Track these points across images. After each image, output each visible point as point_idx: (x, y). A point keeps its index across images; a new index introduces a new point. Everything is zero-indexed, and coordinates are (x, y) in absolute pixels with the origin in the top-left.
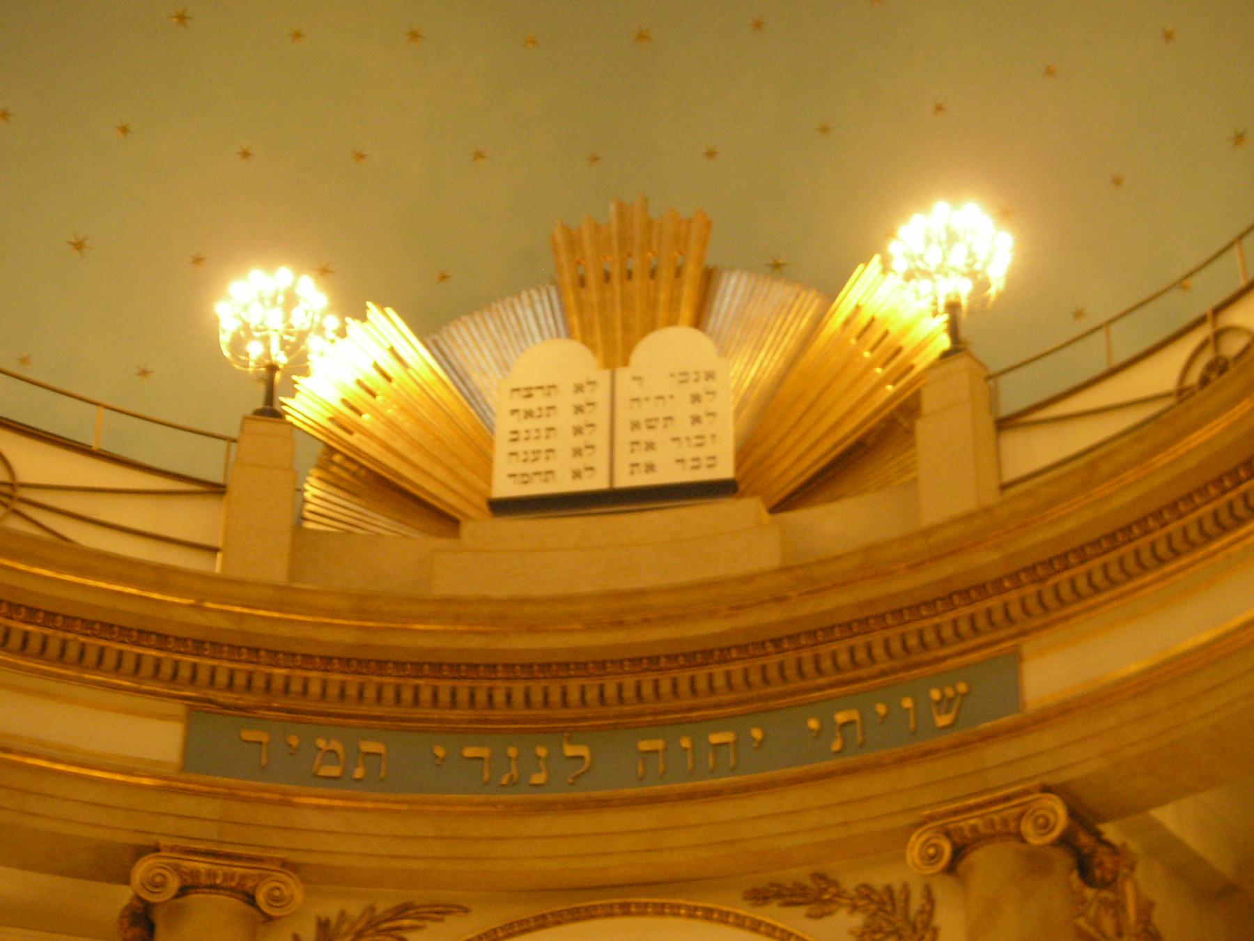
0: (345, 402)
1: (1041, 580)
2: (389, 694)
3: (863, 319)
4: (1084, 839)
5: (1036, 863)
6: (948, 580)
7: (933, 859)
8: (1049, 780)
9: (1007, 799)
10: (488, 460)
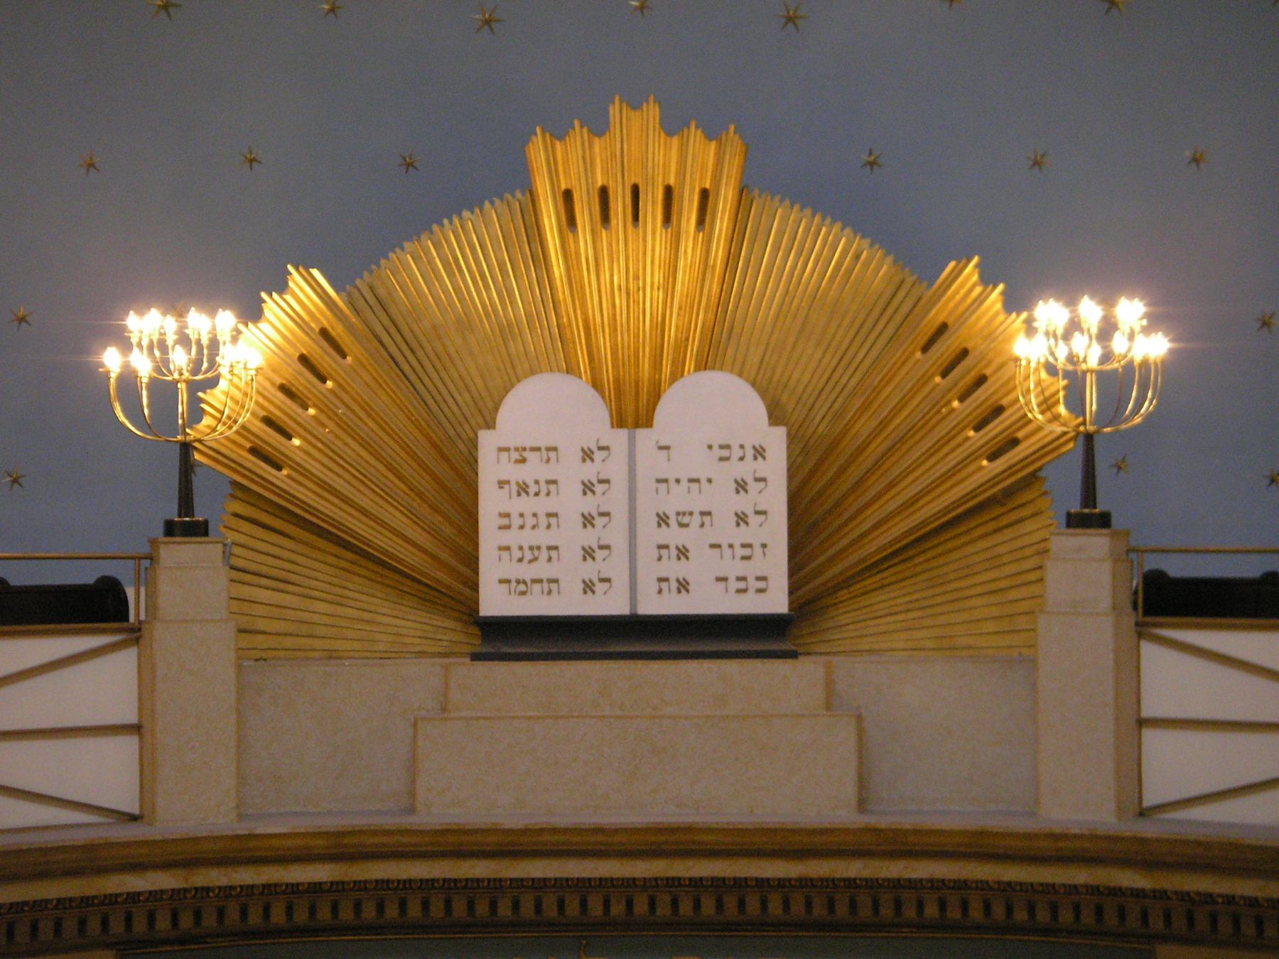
10: (472, 561)
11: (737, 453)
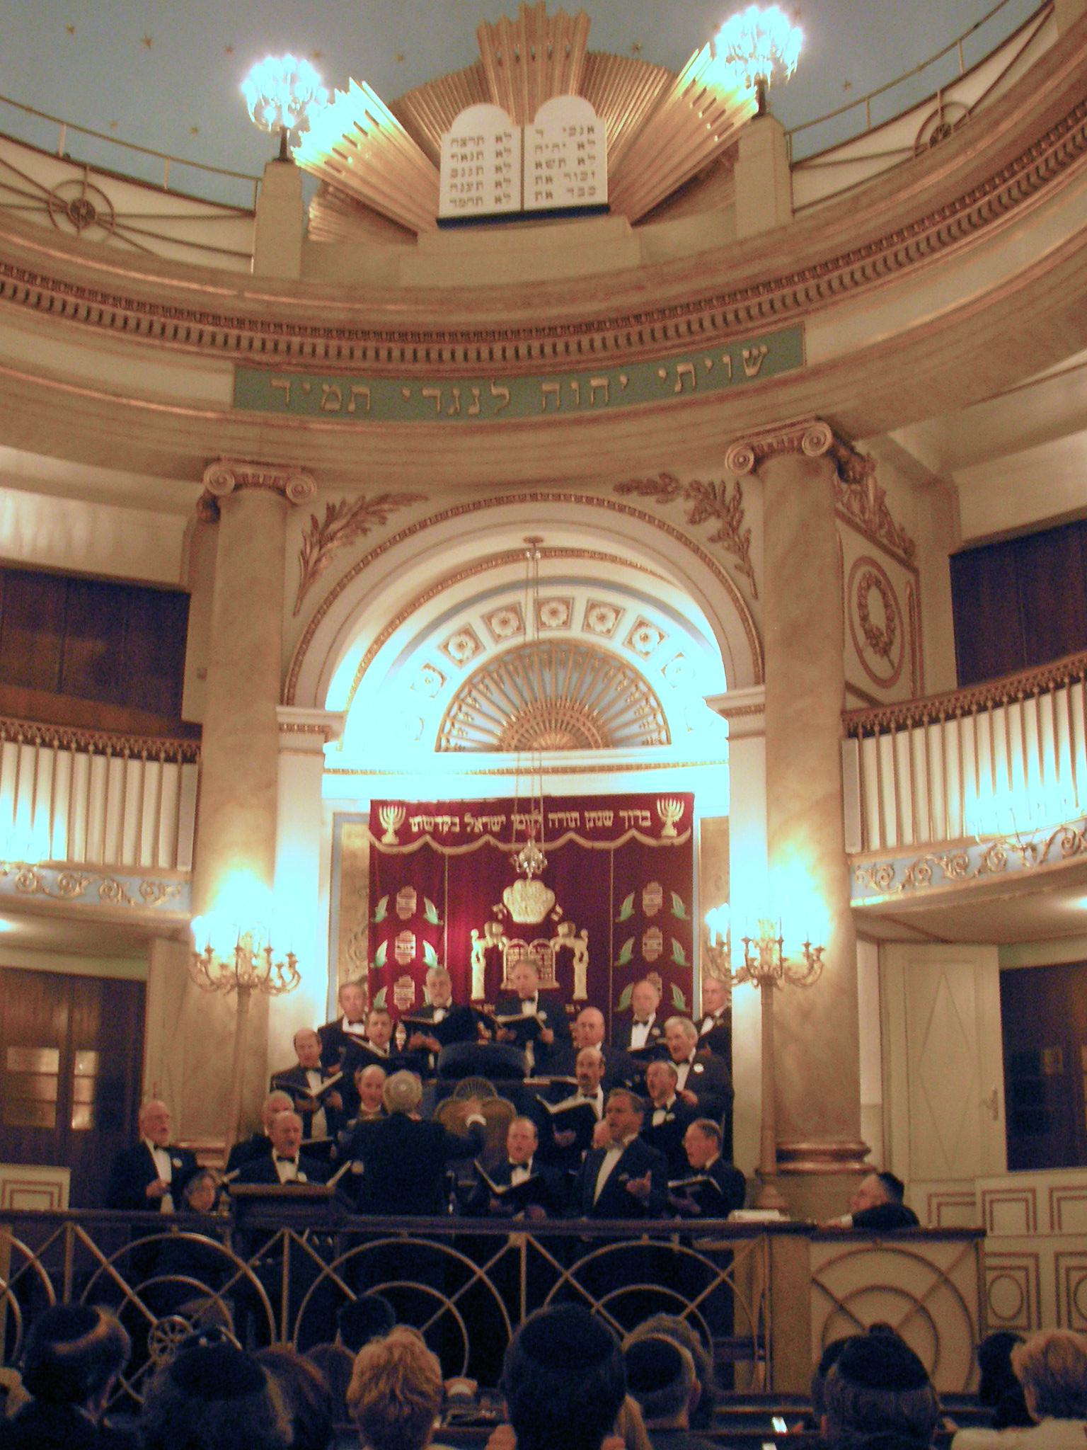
0: (335, 150)
1: (819, 276)
2: (371, 353)
3: (698, 89)
4: (843, 452)
5: (811, 468)
6: (756, 276)
7: (741, 465)
8: (821, 413)
9: (793, 425)
10: (435, 189)
11: (578, 130)
